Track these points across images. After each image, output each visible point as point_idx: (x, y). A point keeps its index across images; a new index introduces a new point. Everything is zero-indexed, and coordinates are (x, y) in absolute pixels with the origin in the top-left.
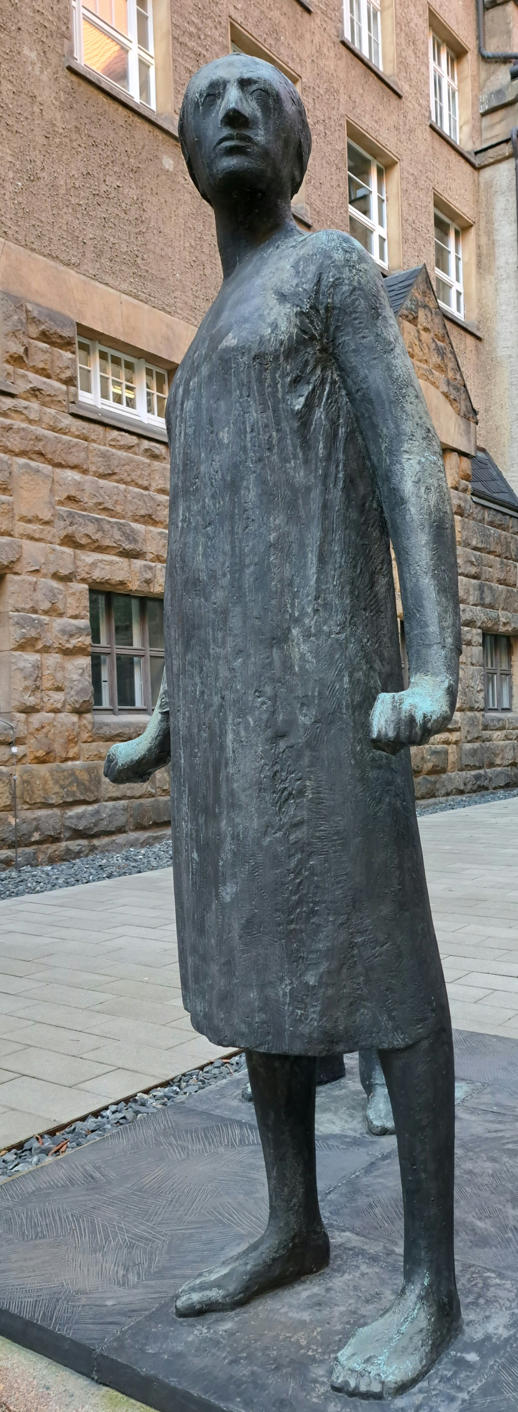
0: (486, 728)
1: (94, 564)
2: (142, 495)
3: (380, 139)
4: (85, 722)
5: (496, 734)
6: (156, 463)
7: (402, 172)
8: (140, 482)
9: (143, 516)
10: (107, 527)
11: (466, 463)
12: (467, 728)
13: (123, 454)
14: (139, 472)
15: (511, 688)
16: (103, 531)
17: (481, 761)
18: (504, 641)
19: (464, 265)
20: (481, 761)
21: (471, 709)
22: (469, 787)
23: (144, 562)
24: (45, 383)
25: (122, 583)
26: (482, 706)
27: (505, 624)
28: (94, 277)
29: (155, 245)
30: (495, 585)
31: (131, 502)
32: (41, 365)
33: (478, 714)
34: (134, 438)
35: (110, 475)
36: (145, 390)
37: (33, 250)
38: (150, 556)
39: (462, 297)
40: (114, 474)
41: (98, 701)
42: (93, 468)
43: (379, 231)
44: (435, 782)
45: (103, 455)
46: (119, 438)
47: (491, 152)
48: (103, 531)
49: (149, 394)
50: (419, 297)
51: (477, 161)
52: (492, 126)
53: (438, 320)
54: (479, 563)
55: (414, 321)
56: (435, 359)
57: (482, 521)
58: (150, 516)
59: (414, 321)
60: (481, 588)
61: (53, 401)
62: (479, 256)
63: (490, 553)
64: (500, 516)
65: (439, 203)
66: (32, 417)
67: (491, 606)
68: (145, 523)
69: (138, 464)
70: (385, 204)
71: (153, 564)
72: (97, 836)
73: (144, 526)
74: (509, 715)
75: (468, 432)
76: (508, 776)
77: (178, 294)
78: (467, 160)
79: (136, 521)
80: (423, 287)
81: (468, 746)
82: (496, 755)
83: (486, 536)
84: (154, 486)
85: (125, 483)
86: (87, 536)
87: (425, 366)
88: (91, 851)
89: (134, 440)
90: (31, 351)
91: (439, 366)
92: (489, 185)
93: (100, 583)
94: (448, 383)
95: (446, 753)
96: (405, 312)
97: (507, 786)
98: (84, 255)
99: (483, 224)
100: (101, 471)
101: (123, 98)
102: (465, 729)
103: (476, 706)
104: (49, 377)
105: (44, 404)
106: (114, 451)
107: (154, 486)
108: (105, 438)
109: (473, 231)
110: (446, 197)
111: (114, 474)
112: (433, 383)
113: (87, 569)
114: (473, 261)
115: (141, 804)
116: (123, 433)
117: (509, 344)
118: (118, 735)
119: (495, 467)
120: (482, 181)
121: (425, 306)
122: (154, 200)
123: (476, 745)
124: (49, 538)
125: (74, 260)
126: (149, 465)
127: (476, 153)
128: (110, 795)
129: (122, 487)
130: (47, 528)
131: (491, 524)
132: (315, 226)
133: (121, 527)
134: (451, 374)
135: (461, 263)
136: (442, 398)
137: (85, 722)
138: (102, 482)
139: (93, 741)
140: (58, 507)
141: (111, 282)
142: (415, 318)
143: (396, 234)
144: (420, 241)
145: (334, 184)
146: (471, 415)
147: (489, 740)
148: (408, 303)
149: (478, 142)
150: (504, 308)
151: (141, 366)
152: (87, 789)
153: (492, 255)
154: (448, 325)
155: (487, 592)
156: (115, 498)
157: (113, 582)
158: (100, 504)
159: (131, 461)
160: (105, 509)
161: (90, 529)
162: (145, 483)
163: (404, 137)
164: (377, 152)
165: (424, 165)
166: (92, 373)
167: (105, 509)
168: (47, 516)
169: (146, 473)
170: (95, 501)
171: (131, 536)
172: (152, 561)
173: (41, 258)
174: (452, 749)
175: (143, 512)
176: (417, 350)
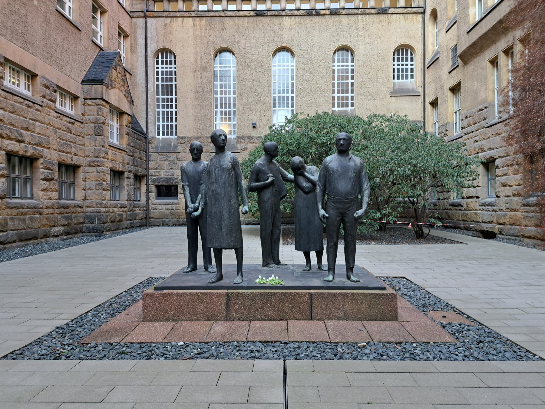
0: (134, 207)
1: (8, 145)
2: (25, 120)
3: (102, 3)
4: (3, 202)
5: (137, 209)
6: (29, 109)
7: (109, 15)
8: (24, 116)
9: (25, 128)
10: (13, 131)
11: (130, 118)
12: (129, 207)
13: (18, 105)
14: (23, 112)
15: (140, 194)
16: (12, 133)
17: (132, 218)
18: (138, 179)
19: (126, 48)
20: (132, 218)
21: (130, 200)
22: (129, 226)
23: (24, 144)
25: (17, 152)
26: (133, 199)
27: (140, 172)
28: (10, 41)
29: (31, 31)
30: (137, 159)
31: (21, 122)
33: (132, 202)
34: (22, 99)
35: (14, 112)
36: (24, 81)
38: (26, 142)
39: (125, 59)
40: (16, 112)
41: (14, 194)
42: (8, 109)
43: (100, 33)
44: (119, 225)
45: (12, 105)
47: (136, 13)
48: (12, 133)
49: (25, 83)
50: (118, 62)
51: (131, 14)
52: (137, 4)
53: (123, 70)
54: (133, 152)
55: (116, 70)
56: (122, 83)
57: (134, 137)
59: (116, 70)
60: (133, 160)
62: (131, 47)
63: (136, 148)
64: (139, 136)
65: (120, 27)
67: (136, 166)
68: (25, 130)
69: (24, 109)
70: (102, 24)
72: (6, 244)
74: (140, 203)
75: (131, 108)
76: (140, 223)
77: (37, 49)
78: (128, 14)
79: (22, 129)
80: (119, 59)
81: (129, 213)
82: (137, 216)
83: (135, 143)
84: (28, 117)
85: (19, 115)
86: (6, 134)
87: (119, 85)
88: (4, 249)
89: (22, 100)
91: (123, 85)
92: (135, 24)
93: (10, 151)
94: (126, 92)
95: (123, 215)
96: (114, 67)
97: (140, 226)
98: (7, 32)
99: (133, 36)
100: (11, 110)
101: (64, 15)
102: (128, 207)
103: (132, 199)
106: (15, 103)
107: (28, 117)
108: (12, 99)
109: (129, 37)
110: (122, 25)
111: (16, 112)
112: (121, 91)
113: (6, 146)
114: (129, 48)
115: (21, 232)
117: (141, 79)
118: (14, 207)
119: (136, 119)
120: (133, 22)
121: (119, 65)
122: (30, 15)
123: (131, 212)
125: (3, 34)
127: (131, 12)
129: (18, 117)
131: (137, 139)
132: (82, 30)
133: (18, 131)
134: (126, 88)
135: (125, 47)
136: (123, 96)
137: (3, 202)
138: (11, 115)
139: (6, 209)
141: (16, 43)
142: (116, 69)
143: (106, 35)
144: (114, 39)
145: (88, 17)
146: (132, 102)
147: (135, 211)
148: (114, 64)
149: (131, 8)
150: (140, 66)
151: (24, 73)
152: (4, 227)
153: (136, 47)
154: (126, 72)
155: (135, 161)
156: (16, 121)
157: (14, 151)
158: (11, 122)
159: (21, 108)
160: (12, 125)
161: (8, 132)
162: (26, 116)
163: (109, 3)
164: (101, 7)
165: (115, 14)
166: (6, 74)
167: (12, 125)
170: (9, 121)
171: (21, 135)
174: (124, 213)
175: (25, 126)
176: (117, 79)
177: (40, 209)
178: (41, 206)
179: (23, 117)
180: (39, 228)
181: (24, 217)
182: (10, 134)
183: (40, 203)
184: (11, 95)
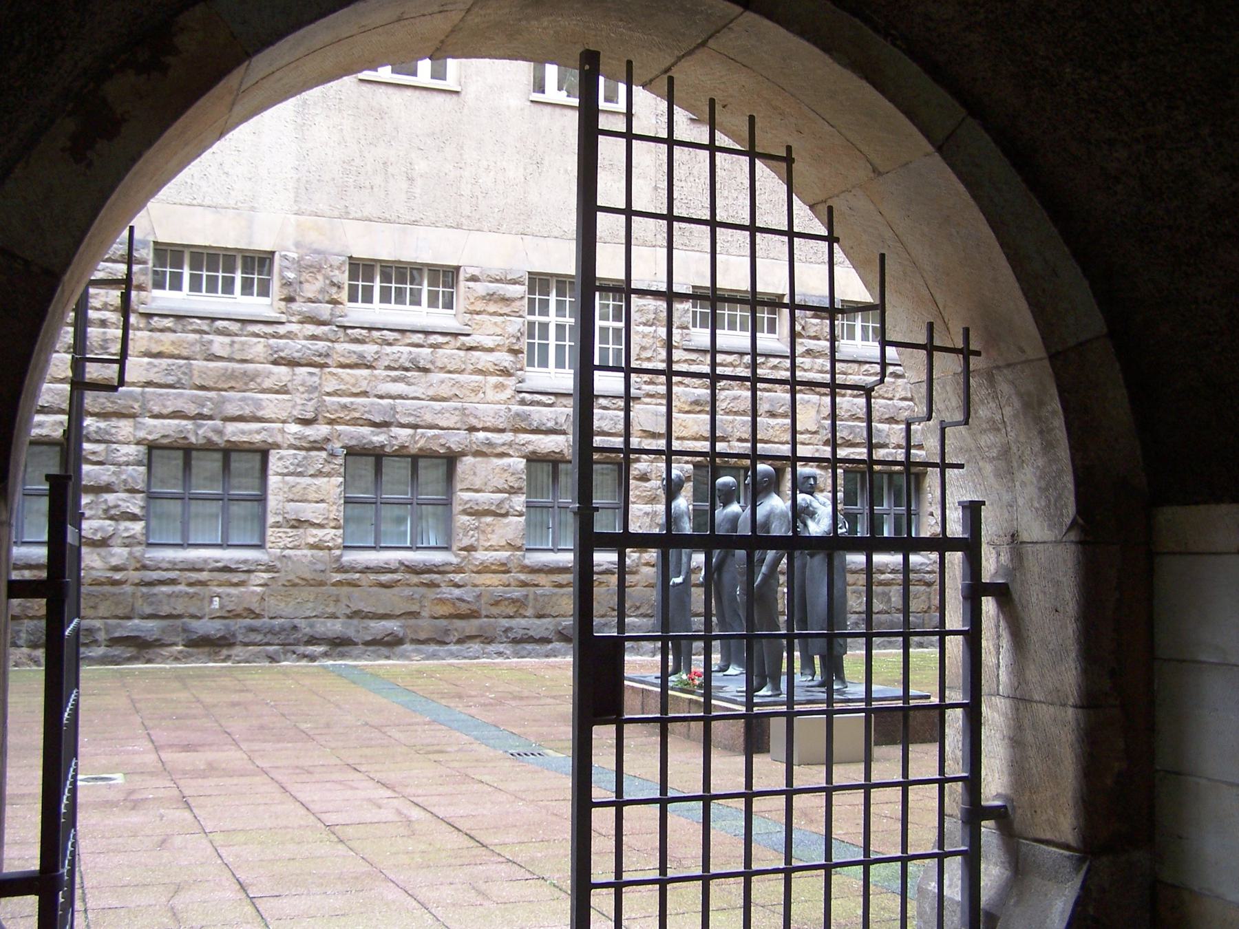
6: (900, 380)
8: (886, 396)
9: (887, 419)
23: (886, 450)
24: (815, 345)
32: (814, 334)
37: (810, 262)
46: (870, 369)
58: (892, 418)
61: (821, 355)
66: (806, 368)
71: (894, 451)
73: (888, 426)
79: (882, 422)
90: (809, 326)
104: (819, 339)
105: (815, 357)
107: (898, 396)
116: (873, 365)
124: (816, 442)
126: (894, 383)
128: (854, 610)
130: (815, 436)
140: (822, 422)
158: (853, 415)
162: (890, 396)
168: (814, 428)
169: (891, 389)
172: (893, 448)
173: (817, 265)
175: (887, 416)
177: (927, 576)
178: (927, 569)
179: (884, 398)
180: (925, 612)
181: (886, 589)
182: (850, 437)
183: (928, 562)
184: (855, 366)
